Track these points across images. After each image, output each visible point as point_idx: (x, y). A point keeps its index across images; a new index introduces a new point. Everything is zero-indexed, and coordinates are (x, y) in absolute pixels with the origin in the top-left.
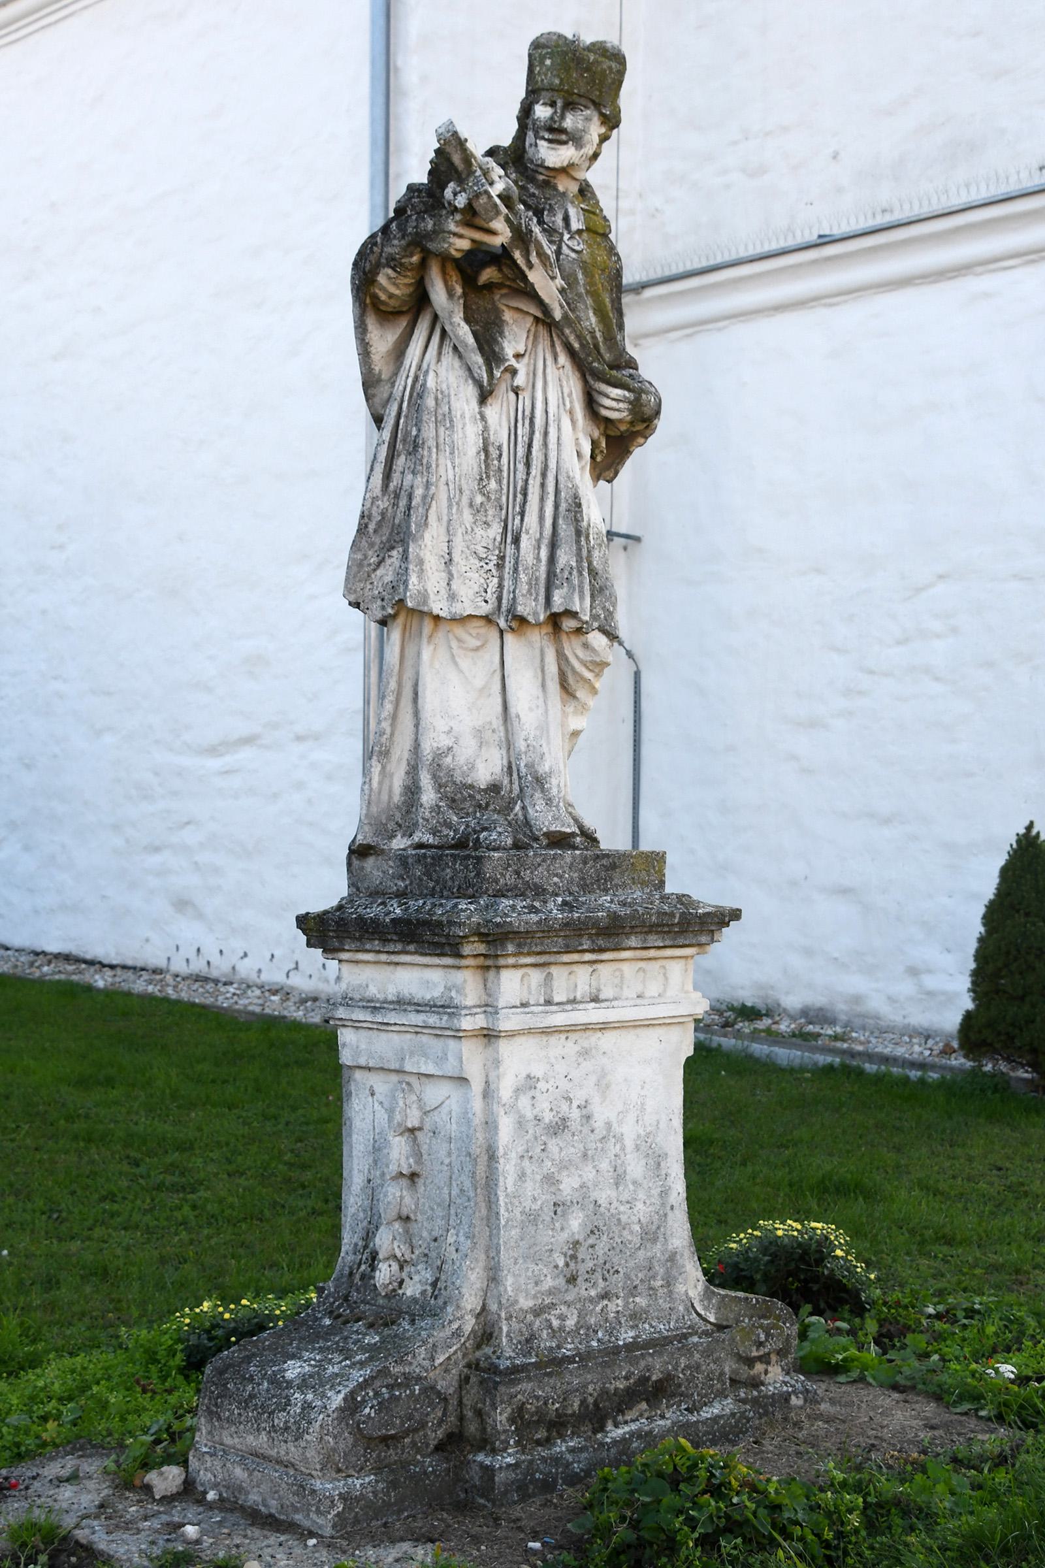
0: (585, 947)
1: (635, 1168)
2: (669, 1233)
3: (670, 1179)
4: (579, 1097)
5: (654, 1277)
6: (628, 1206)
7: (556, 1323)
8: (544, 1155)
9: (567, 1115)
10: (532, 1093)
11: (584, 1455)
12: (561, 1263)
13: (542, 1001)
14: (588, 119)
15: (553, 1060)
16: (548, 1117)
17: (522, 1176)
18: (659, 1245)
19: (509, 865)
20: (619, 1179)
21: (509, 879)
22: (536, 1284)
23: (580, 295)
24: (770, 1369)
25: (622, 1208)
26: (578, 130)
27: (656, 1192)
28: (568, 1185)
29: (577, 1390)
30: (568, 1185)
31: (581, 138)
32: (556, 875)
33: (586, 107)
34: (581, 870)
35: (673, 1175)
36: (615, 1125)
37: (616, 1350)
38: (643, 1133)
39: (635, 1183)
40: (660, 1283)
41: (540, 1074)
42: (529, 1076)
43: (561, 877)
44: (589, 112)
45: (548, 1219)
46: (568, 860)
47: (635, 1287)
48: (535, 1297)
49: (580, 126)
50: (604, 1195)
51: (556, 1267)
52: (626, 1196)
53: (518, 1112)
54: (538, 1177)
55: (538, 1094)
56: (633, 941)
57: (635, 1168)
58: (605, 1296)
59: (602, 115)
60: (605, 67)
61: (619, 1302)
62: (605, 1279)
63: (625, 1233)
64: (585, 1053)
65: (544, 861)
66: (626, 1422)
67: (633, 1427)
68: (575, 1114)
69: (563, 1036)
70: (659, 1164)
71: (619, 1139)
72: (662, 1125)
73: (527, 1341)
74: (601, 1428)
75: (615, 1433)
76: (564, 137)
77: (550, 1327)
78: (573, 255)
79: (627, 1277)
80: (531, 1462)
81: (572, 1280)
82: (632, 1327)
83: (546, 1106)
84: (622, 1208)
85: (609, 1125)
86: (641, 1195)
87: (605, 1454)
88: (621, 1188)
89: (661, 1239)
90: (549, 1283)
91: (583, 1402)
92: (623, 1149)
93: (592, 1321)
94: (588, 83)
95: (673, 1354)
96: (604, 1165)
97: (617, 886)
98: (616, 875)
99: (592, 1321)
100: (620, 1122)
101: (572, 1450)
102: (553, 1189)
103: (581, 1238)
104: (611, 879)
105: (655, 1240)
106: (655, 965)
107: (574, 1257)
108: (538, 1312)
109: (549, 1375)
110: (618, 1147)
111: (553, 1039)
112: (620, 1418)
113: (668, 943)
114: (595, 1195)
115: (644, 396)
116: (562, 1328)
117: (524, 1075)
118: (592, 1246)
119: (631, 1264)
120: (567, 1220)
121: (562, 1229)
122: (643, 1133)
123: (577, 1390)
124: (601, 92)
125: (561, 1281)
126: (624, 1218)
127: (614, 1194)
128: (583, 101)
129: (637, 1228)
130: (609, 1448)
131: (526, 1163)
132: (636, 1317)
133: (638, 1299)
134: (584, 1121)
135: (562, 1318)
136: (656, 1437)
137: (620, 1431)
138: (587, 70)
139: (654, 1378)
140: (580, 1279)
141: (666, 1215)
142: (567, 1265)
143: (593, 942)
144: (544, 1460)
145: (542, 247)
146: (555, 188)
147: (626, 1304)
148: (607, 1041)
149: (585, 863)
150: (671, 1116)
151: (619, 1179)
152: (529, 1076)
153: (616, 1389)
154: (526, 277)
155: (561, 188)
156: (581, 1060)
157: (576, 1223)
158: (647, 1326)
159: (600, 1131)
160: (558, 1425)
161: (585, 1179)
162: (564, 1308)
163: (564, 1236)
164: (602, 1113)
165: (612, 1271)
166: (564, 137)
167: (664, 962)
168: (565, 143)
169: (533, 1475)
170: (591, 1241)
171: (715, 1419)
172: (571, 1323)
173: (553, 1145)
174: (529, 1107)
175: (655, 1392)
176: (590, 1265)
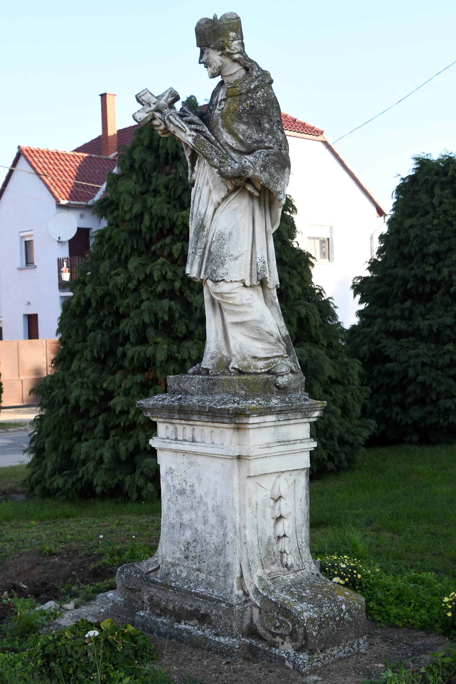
0: (176, 417)
1: (212, 519)
2: (227, 554)
3: (227, 530)
4: (190, 481)
5: (219, 571)
6: (209, 535)
7: (178, 572)
8: (177, 502)
9: (185, 488)
10: (172, 475)
11: (165, 627)
12: (183, 549)
13: (174, 438)
14: (208, 53)
15: (179, 464)
16: (178, 487)
17: (169, 508)
18: (222, 558)
19: (175, 381)
20: (205, 522)
21: (176, 387)
22: (173, 553)
23: (219, 129)
24: (285, 643)
25: (207, 535)
27: (221, 533)
28: (186, 517)
29: (172, 601)
30: (186, 517)
31: (208, 62)
32: (193, 386)
34: (202, 385)
35: (229, 528)
36: (204, 498)
37: (191, 593)
38: (216, 505)
39: (212, 526)
40: (221, 575)
41: (174, 468)
42: (170, 468)
43: (195, 387)
45: (178, 529)
46: (197, 380)
47: (211, 572)
48: (172, 558)
49: (206, 58)
50: (200, 527)
51: (181, 550)
52: (208, 530)
53: (167, 482)
54: (175, 511)
55: (174, 476)
56: (195, 417)
57: (212, 519)
58: (199, 570)
59: (214, 48)
60: (203, 29)
61: (204, 575)
62: (199, 563)
63: (208, 546)
64: (191, 463)
65: (188, 380)
66: (189, 625)
67: (190, 628)
68: (188, 488)
69: (182, 454)
70: (223, 521)
71: (206, 504)
72: (224, 504)
73: (167, 574)
74: (179, 622)
75: (182, 626)
77: (176, 573)
78: (219, 112)
79: (208, 566)
80: (147, 618)
81: (187, 557)
82: (205, 588)
83: (177, 482)
84: (207, 535)
85: (201, 497)
86: (215, 532)
87: (172, 631)
88: (206, 526)
89: (223, 555)
90: (178, 555)
91: (174, 607)
92: (207, 509)
93: (192, 578)
95: (210, 606)
96: (200, 514)
97: (216, 392)
98: (216, 387)
99: (192, 578)
100: (206, 497)
101: (162, 623)
102: (180, 517)
103: (190, 541)
104: (214, 389)
105: (220, 555)
106: (218, 431)
107: (187, 548)
108: (173, 565)
109: (162, 589)
110: (205, 507)
111: (179, 455)
112: (187, 621)
113: (210, 420)
114: (196, 525)
115: (222, 169)
116: (180, 575)
117: (168, 467)
118: (195, 547)
119: (210, 561)
120: (185, 532)
121: (183, 535)
122: (216, 505)
123: (172, 601)
124: (205, 41)
125: (182, 557)
126: (207, 540)
127: (203, 528)
129: (213, 546)
130: (174, 630)
131: (170, 503)
132: (209, 584)
133: (211, 578)
134: (192, 492)
135: (181, 571)
136: (193, 636)
137: (184, 626)
139: (202, 612)
140: (189, 558)
141: (225, 545)
142: (185, 551)
143: (179, 416)
144: (152, 621)
147: (207, 577)
148: (200, 460)
149: (204, 382)
150: (228, 501)
151: (205, 522)
152: (170, 468)
153: (187, 608)
156: (190, 466)
157: (188, 534)
158: (211, 590)
159: (198, 499)
160: (164, 612)
161: (192, 517)
162: (182, 568)
163: (183, 538)
164: (199, 491)
165: (202, 561)
167: (222, 429)
169: (147, 624)
170: (194, 544)
171: (219, 643)
172: (184, 575)
173: (180, 499)
174: (171, 481)
175: (204, 619)
176: (194, 554)
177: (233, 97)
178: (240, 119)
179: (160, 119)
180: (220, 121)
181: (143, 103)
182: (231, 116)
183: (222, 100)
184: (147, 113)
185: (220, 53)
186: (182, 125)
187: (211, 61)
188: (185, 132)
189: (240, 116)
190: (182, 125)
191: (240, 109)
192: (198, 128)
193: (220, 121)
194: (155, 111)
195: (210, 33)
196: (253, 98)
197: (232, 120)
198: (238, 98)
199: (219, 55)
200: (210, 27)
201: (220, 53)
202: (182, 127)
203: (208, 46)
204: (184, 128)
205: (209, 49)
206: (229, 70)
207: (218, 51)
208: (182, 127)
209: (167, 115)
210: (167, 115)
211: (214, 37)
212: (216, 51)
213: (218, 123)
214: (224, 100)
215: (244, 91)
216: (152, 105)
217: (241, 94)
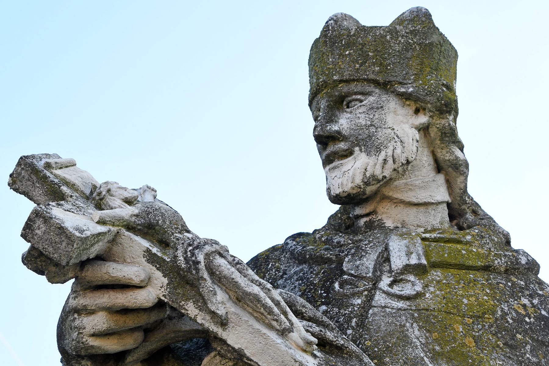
26: (361, 127)
33: (366, 94)
44: (371, 99)
76: (342, 146)
78: (401, 304)
94: (356, 61)
124: (381, 65)
128: (353, 87)
138: (348, 45)
145: (236, 285)
146: (381, 226)
154: (223, 342)
155: (389, 224)
166: (342, 146)
168: (348, 153)
177: (455, 271)
178: (511, 347)
179: (151, 258)
180: (415, 333)
181: (64, 188)
182: (469, 329)
183: (408, 269)
184: (101, 222)
185: (423, 119)
186: (277, 304)
187: (381, 134)
188: (284, 333)
189: (513, 337)
190: (277, 304)
191: (504, 314)
192: (330, 335)
193: (415, 333)
194: (130, 228)
195: (408, 47)
196: (539, 295)
197: (477, 340)
198: (480, 277)
199: (416, 128)
200: (414, 33)
201: (423, 119)
202: (276, 310)
203: (385, 86)
204: (285, 314)
205: (384, 97)
206: (424, 187)
207: (417, 111)
208: (276, 310)
209: (208, 248)
210: (208, 248)
211: (422, 63)
212: (411, 112)
213: (405, 340)
214: (419, 270)
215: (500, 263)
216: (116, 202)
217: (487, 269)
